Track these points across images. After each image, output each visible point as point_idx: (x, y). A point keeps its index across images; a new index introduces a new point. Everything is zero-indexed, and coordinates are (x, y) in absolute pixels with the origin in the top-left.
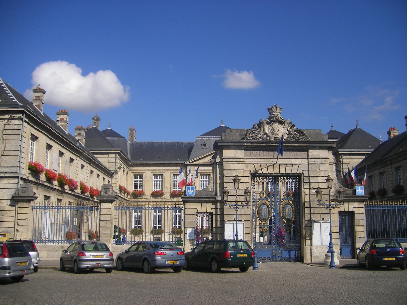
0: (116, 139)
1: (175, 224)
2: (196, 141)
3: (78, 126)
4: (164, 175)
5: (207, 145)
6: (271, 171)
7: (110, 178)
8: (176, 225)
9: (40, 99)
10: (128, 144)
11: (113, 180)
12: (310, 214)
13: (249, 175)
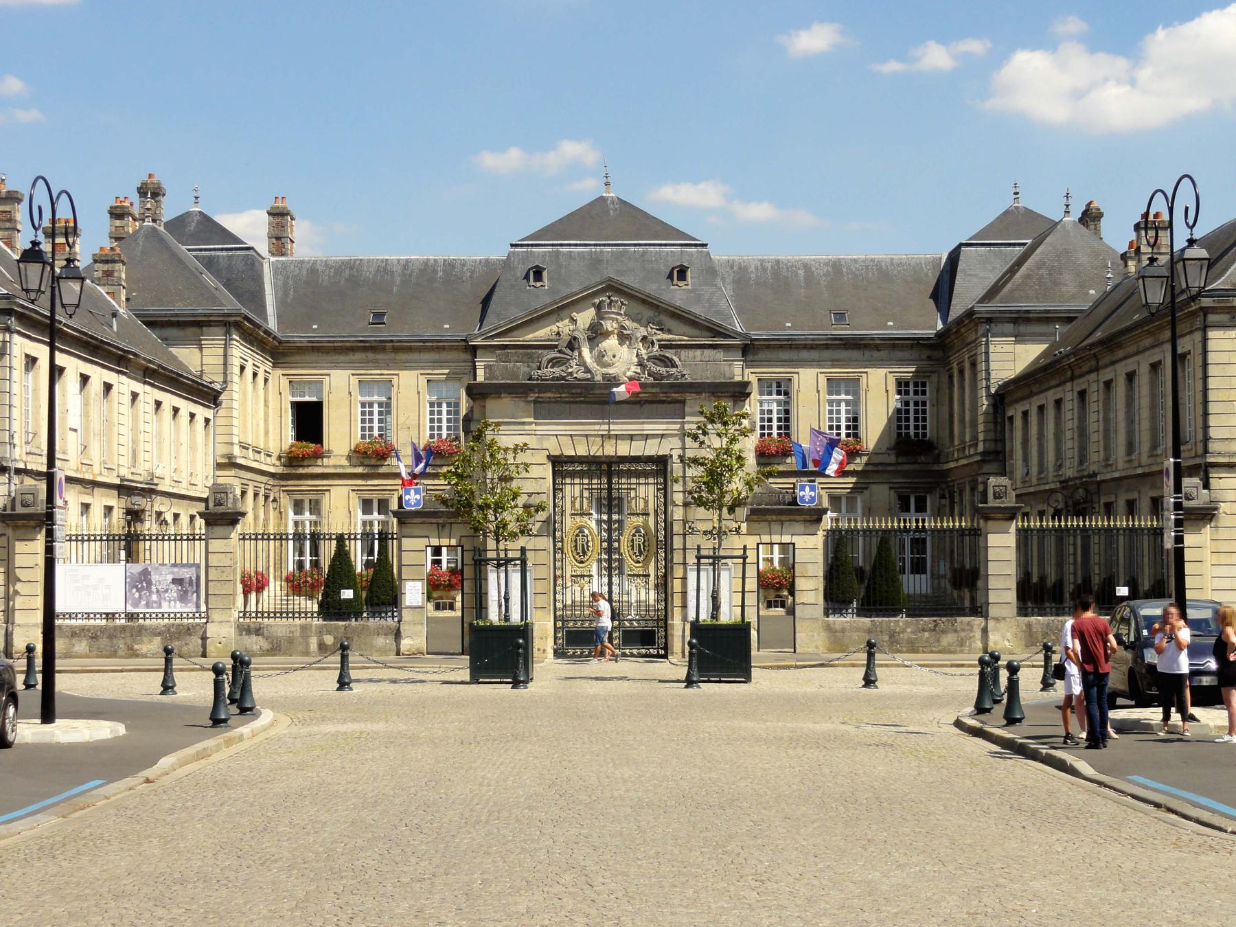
0: (224, 253)
2: (509, 257)
3: (102, 249)
4: (395, 382)
5: (545, 274)
6: (596, 451)
7: (209, 407)
9: (10, 220)
10: (266, 269)
11: (222, 412)
12: (684, 549)
13: (545, 460)
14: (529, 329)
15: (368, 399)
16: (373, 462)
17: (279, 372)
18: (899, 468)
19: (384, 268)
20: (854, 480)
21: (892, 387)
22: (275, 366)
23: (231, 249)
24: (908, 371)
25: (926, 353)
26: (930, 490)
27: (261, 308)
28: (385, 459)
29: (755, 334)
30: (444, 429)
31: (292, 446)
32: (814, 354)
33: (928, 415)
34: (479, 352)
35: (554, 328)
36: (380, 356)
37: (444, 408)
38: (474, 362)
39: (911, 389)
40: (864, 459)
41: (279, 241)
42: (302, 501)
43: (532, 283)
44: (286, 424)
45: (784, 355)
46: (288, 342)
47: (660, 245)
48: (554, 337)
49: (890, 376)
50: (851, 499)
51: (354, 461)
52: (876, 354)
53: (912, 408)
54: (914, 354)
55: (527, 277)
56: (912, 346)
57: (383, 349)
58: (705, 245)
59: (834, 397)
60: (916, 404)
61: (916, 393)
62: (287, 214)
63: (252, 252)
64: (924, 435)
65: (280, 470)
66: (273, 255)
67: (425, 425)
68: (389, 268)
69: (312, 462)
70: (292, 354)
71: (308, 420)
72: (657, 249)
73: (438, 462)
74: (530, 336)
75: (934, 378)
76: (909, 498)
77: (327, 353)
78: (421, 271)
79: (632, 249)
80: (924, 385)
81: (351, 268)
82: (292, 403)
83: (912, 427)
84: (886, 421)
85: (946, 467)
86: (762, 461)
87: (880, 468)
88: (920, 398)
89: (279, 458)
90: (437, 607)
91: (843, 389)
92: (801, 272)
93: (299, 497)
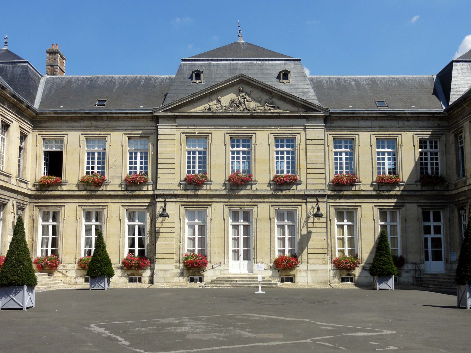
0: (10, 65)
1: (132, 245)
2: (180, 66)
4: (108, 139)
5: (202, 75)
8: (43, 238)
10: (43, 81)
14: (192, 106)
15: (91, 150)
16: (93, 188)
17: (37, 132)
18: (424, 193)
19: (111, 81)
20: (395, 201)
21: (417, 144)
22: (34, 128)
23: (14, 63)
24: (427, 133)
25: (437, 122)
26: (443, 207)
27: (32, 97)
28: (100, 186)
29: (332, 109)
30: (138, 168)
31: (42, 178)
32: (368, 123)
33: (439, 161)
34: (160, 120)
35: (207, 106)
36: (99, 123)
37: (139, 155)
38: (157, 127)
39: (428, 145)
40: (401, 188)
41: (52, 67)
42: (48, 212)
43: (194, 81)
44: (40, 165)
45: (349, 123)
46: (42, 114)
47: (272, 60)
48: (207, 111)
49: (416, 137)
50: (393, 214)
51: (81, 187)
52: (406, 123)
53: (429, 157)
54: (430, 123)
55: (191, 77)
56: (428, 119)
57: (101, 119)
58: (300, 60)
59: (381, 150)
60: (431, 154)
61: (431, 147)
62: (58, 52)
63: (27, 64)
64: (437, 173)
65: (34, 193)
66: (48, 75)
67: (126, 165)
68: (113, 80)
69: (55, 187)
70: (45, 122)
71: (54, 162)
72: (270, 62)
73: (134, 188)
74: (192, 110)
75: (443, 138)
76: (429, 212)
77: (67, 121)
78: (131, 82)
79: (255, 62)
80: (436, 143)
81: (92, 81)
82: (46, 153)
83: (429, 169)
84: (413, 164)
85: (453, 192)
86: (337, 188)
87: (412, 193)
88: (434, 151)
89: (34, 185)
90: (131, 281)
91: (386, 145)
92: (353, 83)
93: (46, 210)
